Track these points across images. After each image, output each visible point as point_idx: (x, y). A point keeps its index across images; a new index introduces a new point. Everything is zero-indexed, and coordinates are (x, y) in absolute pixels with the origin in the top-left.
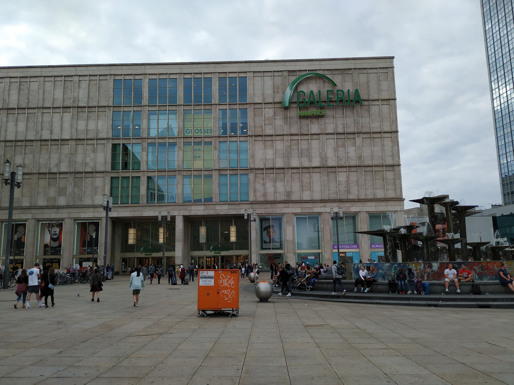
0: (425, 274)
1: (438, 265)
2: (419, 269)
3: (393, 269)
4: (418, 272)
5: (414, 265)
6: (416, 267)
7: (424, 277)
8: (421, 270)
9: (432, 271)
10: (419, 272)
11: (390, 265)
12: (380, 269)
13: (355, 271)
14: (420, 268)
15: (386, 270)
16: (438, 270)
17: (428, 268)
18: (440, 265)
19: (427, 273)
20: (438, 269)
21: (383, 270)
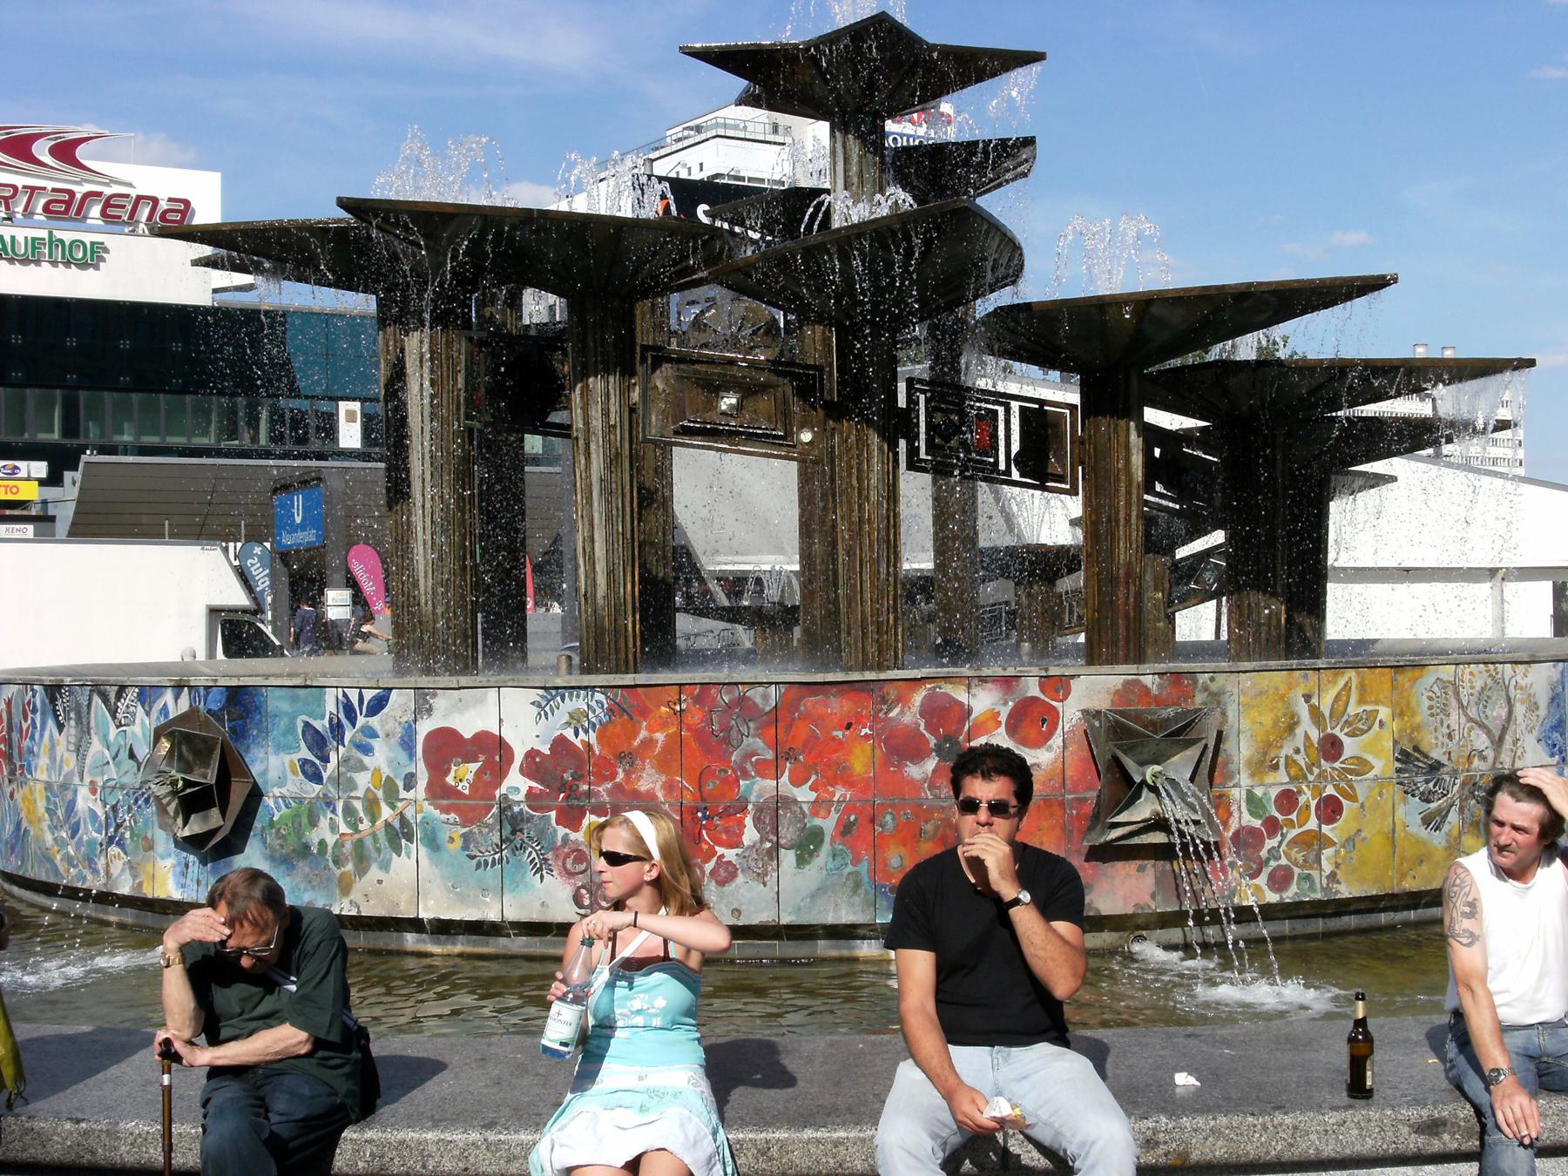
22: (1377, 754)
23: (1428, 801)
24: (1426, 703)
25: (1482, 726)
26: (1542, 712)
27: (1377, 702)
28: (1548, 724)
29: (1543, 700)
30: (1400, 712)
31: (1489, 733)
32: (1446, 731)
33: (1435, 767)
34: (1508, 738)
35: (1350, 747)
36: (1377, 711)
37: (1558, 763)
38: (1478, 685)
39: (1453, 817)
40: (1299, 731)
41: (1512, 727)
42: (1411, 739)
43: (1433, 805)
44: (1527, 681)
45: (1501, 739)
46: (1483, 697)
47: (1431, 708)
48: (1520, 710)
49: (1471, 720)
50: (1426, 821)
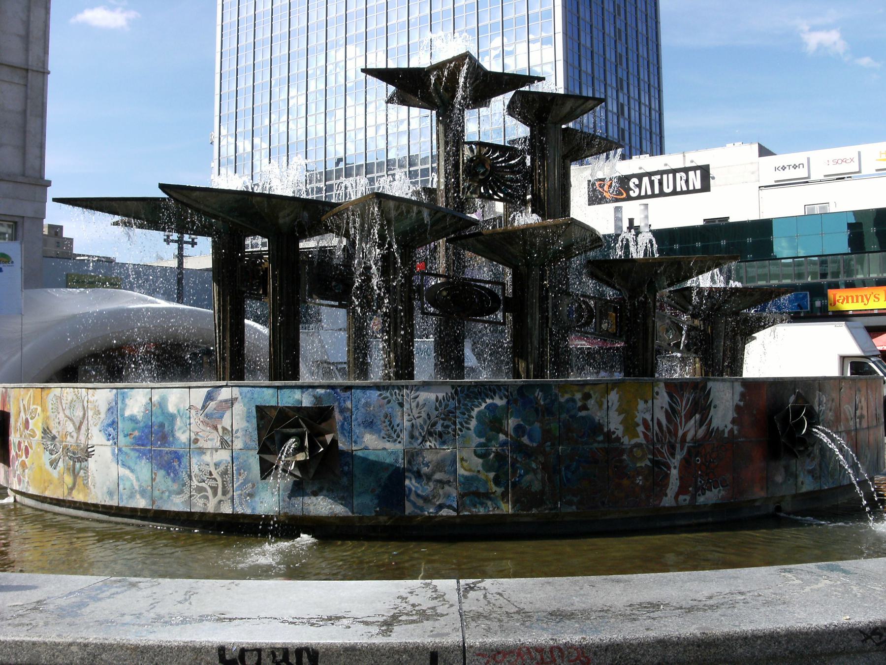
0: (673, 455)
1: (737, 397)
2: (645, 421)
3: (473, 423)
4: (638, 445)
6: (627, 411)
7: (667, 476)
8: (656, 427)
9: (709, 433)
10: (641, 439)
12: (369, 425)
13: (122, 440)
14: (648, 417)
15: (417, 434)
16: (735, 428)
17: (689, 417)
18: (743, 396)
19: (682, 449)
20: (733, 421)
24: (51, 406)
25: (71, 420)
26: (103, 416)
27: (37, 405)
29: (103, 409)
31: (74, 424)
32: (58, 421)
33: (54, 438)
34: (84, 428)
36: (37, 409)
37: (112, 445)
38: (70, 398)
39: (61, 464)
41: (85, 422)
42: (46, 423)
43: (53, 457)
44: (95, 398)
45: (79, 428)
46: (72, 406)
48: (90, 413)
49: (66, 416)
50: (51, 464)
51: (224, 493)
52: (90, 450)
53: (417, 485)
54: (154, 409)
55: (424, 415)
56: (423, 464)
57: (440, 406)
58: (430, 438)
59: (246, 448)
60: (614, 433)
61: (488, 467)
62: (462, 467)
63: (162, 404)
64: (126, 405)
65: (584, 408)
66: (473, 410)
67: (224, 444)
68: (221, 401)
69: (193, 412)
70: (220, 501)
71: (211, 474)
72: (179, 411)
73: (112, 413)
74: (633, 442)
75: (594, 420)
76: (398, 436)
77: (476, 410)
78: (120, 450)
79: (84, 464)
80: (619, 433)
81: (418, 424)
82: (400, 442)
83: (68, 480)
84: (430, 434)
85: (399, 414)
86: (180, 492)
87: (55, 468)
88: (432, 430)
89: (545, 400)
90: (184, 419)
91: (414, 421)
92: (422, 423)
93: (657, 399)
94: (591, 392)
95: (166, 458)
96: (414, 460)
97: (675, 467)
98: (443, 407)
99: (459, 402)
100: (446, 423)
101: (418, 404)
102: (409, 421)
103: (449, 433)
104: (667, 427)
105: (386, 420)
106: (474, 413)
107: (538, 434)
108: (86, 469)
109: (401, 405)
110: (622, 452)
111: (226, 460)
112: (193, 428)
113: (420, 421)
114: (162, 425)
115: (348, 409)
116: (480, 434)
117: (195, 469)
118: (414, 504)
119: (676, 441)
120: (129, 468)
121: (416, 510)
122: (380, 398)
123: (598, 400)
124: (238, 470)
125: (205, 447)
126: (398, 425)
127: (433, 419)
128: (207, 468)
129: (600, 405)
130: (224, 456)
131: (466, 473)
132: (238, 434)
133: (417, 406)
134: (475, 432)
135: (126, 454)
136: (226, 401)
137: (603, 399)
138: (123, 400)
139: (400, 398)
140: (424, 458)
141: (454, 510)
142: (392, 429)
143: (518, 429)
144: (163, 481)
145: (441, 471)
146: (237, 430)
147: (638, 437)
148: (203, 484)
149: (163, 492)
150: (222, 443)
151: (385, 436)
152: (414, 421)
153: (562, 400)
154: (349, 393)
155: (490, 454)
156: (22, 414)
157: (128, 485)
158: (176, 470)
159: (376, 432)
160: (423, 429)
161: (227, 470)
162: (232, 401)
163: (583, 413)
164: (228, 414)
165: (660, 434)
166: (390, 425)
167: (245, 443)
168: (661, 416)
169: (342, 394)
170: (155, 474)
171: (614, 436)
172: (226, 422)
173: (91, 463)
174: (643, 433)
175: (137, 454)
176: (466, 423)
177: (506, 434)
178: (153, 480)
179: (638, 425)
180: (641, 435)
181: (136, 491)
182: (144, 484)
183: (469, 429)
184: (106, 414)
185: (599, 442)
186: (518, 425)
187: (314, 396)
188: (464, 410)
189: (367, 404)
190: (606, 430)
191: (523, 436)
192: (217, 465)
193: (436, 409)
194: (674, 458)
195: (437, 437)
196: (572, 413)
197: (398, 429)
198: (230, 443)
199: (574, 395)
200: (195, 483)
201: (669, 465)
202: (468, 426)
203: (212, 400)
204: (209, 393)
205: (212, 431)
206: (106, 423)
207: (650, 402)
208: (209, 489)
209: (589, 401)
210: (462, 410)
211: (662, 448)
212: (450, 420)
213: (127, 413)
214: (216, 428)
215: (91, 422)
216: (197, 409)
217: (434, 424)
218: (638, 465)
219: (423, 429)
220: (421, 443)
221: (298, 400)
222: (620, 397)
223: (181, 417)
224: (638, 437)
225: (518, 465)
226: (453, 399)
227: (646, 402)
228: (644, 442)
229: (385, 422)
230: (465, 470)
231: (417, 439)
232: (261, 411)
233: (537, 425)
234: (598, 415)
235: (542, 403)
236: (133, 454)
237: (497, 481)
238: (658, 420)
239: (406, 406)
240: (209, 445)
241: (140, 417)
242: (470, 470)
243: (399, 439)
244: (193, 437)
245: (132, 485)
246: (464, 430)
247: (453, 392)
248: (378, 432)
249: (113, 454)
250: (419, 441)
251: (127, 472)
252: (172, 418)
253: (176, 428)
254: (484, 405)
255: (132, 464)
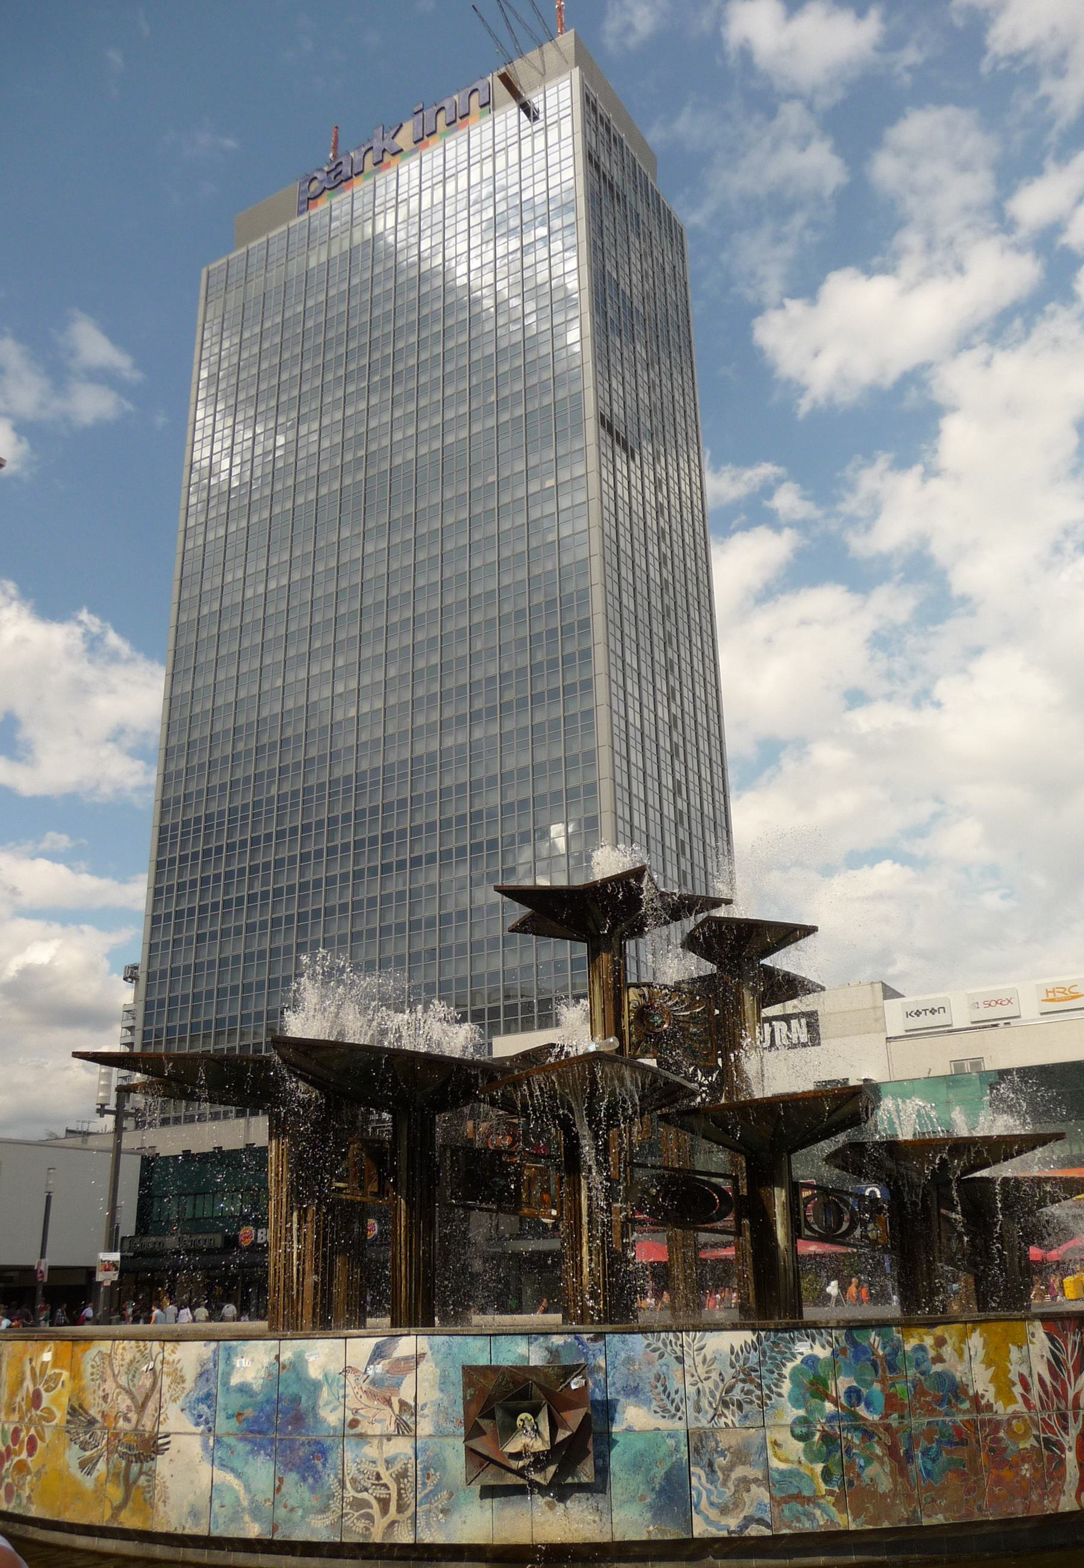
0: (1065, 1428)
3: (786, 1386)
4: (1016, 1415)
5: (976, 1341)
6: (995, 1359)
7: (1062, 1462)
10: (1019, 1407)
11: (746, 1348)
12: (633, 1391)
14: (1026, 1373)
21: (670, 1406)
22: (59, 1406)
23: (84, 1449)
24: (90, 1370)
25: (129, 1392)
26: (189, 1384)
27: (62, 1367)
28: (195, 1395)
29: (190, 1372)
30: (76, 1375)
31: (133, 1398)
32: (101, 1393)
33: (92, 1422)
34: (151, 1405)
35: (46, 1398)
36: (61, 1374)
37: (202, 1434)
38: (128, 1357)
39: (101, 1466)
40: (25, 1385)
41: (156, 1395)
42: (78, 1398)
43: (88, 1453)
44: (175, 1357)
45: (144, 1405)
46: (132, 1368)
47: (92, 1374)
48: (166, 1381)
49: (119, 1386)
50: (82, 1465)
51: (400, 1509)
52: (160, 1442)
53: (709, 1486)
54: (283, 1373)
55: (715, 1376)
56: (717, 1452)
57: (737, 1361)
58: (726, 1412)
59: (440, 1434)
60: (983, 1396)
61: (813, 1456)
62: (775, 1455)
63: (297, 1366)
64: (234, 1367)
65: (939, 1359)
66: (784, 1365)
67: (403, 1429)
68: (398, 1360)
69: (351, 1377)
70: (393, 1523)
71: (378, 1477)
72: (326, 1376)
73: (208, 1380)
74: (1011, 1409)
75: (954, 1377)
76: (678, 1409)
77: (790, 1365)
78: (217, 1441)
79: (146, 1466)
80: (990, 1396)
81: (707, 1391)
82: (680, 1419)
83: (115, 1493)
84: (725, 1404)
85: (679, 1374)
86: (325, 1509)
87: (89, 1473)
88: (728, 1399)
89: (884, 1348)
90: (335, 1389)
91: (700, 1385)
92: (713, 1387)
93: (1033, 1343)
94: (946, 1336)
95: (301, 1454)
96: (703, 1447)
97: (1070, 1448)
98: (741, 1362)
99: (764, 1353)
100: (748, 1386)
101: (705, 1357)
102: (692, 1385)
103: (751, 1402)
104: (1053, 1387)
105: (659, 1385)
106: (786, 1371)
107: (879, 1400)
108: (151, 1474)
109: (680, 1360)
110: (996, 1426)
111: (405, 1454)
112: (351, 1402)
113: (708, 1385)
114: (296, 1399)
115: (600, 1367)
116: (796, 1402)
117: (351, 1470)
118: (707, 1519)
119: (1067, 1407)
120: (233, 1470)
121: (710, 1529)
122: (648, 1350)
123: (957, 1346)
124: (426, 1469)
125: (370, 1433)
126: (677, 1392)
127: (729, 1381)
128: (371, 1468)
129: (960, 1353)
130: (402, 1447)
131: (783, 1466)
132: (426, 1411)
133: (704, 1361)
134: (789, 1397)
135: (229, 1447)
136: (406, 1359)
137: (963, 1346)
138: (229, 1358)
139: (678, 1349)
140: (717, 1443)
141: (768, 1526)
142: (668, 1397)
143: (853, 1394)
144: (296, 1490)
145: (744, 1464)
146: (425, 1405)
147: (1016, 1402)
148: (365, 1495)
149: (292, 1510)
150: (398, 1426)
151: (658, 1410)
152: (700, 1385)
153: (908, 1347)
154: (601, 1343)
155: (813, 1434)
156: (28, 1384)
157: (228, 1500)
158: (317, 1472)
159: (645, 1404)
160: (713, 1397)
161: (406, 1470)
162: (418, 1358)
163: (938, 1368)
164: (409, 1381)
165: (1044, 1397)
166: (664, 1391)
167: (437, 1426)
168: (1041, 1368)
169: (591, 1345)
170: (281, 1480)
171: (983, 1402)
172: (406, 1392)
173: (162, 1464)
174: (1023, 1395)
175: (248, 1448)
176: (776, 1386)
177: (835, 1402)
178: (277, 1490)
179: (1014, 1384)
180: (1020, 1399)
181: (243, 1510)
182: (260, 1498)
183: (780, 1395)
184: (196, 1381)
185: (965, 1412)
186: (849, 1388)
187: (547, 1349)
188: (771, 1367)
189: (629, 1360)
190: (971, 1392)
191: (858, 1405)
192: (388, 1462)
193: (732, 1366)
194: (1067, 1434)
195: (735, 1408)
196: (923, 1368)
197: (677, 1398)
198: (413, 1426)
199: (922, 1340)
200: (350, 1493)
201: (1062, 1445)
202: (779, 1390)
203: (383, 1358)
204: (378, 1347)
205: (384, 1407)
206: (196, 1396)
207: (1025, 1348)
208: (374, 1503)
209: (944, 1348)
210: (770, 1366)
211: (1049, 1417)
212: (752, 1381)
213: (235, 1381)
214: (389, 1402)
215: (166, 1396)
216: (358, 1371)
217: (729, 1390)
218: (1021, 1446)
219: (713, 1397)
220: (713, 1418)
221: (523, 1356)
222: (985, 1341)
223: (330, 1386)
224: (1016, 1402)
225: (854, 1451)
226: (755, 1350)
227: (1020, 1347)
228: (1025, 1410)
229: (656, 1387)
230: (780, 1460)
231: (706, 1412)
232: (471, 1373)
233: (877, 1387)
234: (959, 1372)
235: (881, 1353)
236: (241, 1447)
237: (827, 1475)
238: (1039, 1375)
239: (688, 1361)
240: (377, 1429)
241: (257, 1385)
242: (786, 1461)
243: (679, 1414)
244: (350, 1416)
245: (237, 1498)
246: (774, 1396)
247: (755, 1339)
248: (647, 1402)
249: (205, 1446)
250: (709, 1416)
251: (230, 1478)
252: (316, 1386)
253: (321, 1402)
254: (800, 1358)
255: (237, 1464)
